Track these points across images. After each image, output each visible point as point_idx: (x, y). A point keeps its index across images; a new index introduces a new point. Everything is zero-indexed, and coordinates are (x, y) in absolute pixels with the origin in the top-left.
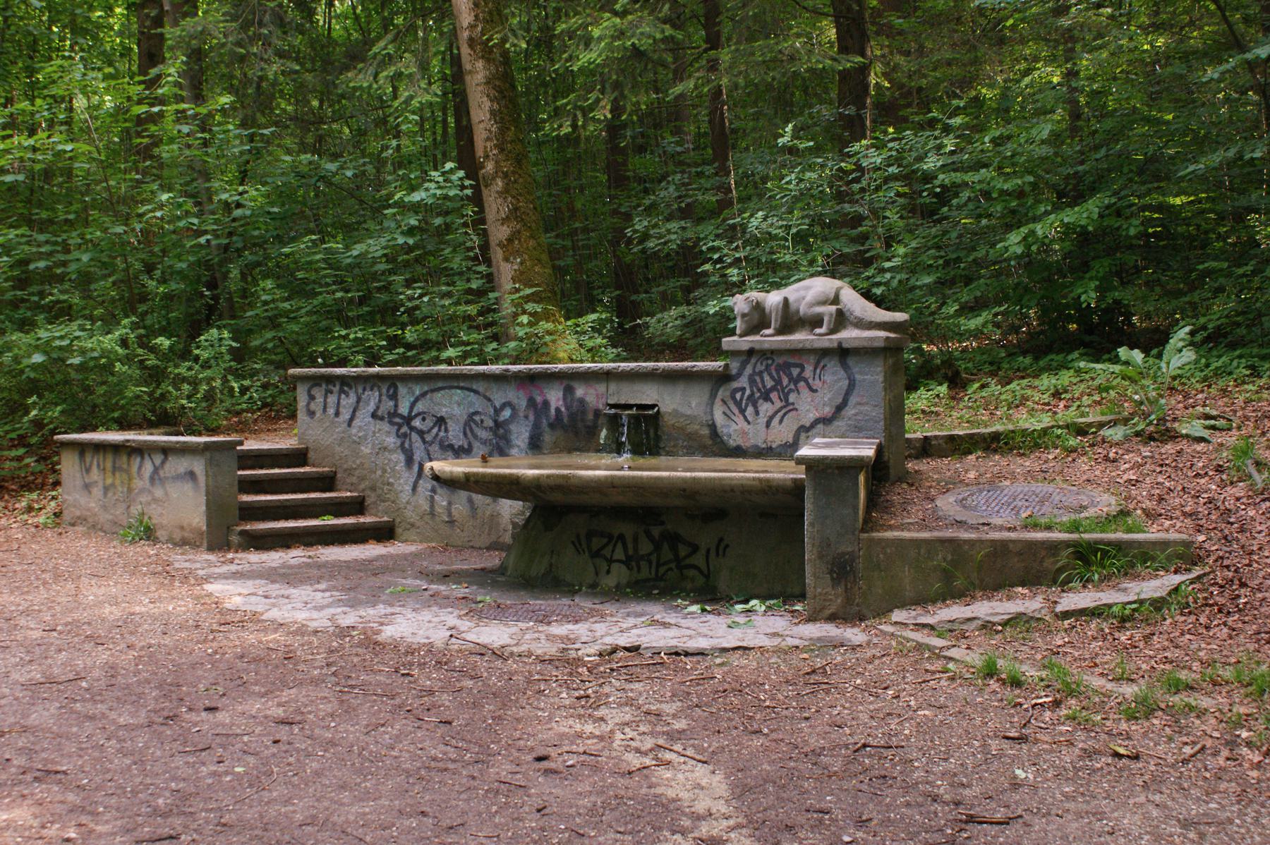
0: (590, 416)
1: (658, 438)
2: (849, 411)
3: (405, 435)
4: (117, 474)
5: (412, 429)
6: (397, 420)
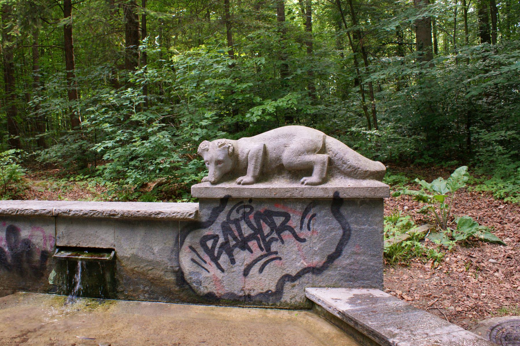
0: (37, 257)
1: (115, 282)
2: (343, 261)
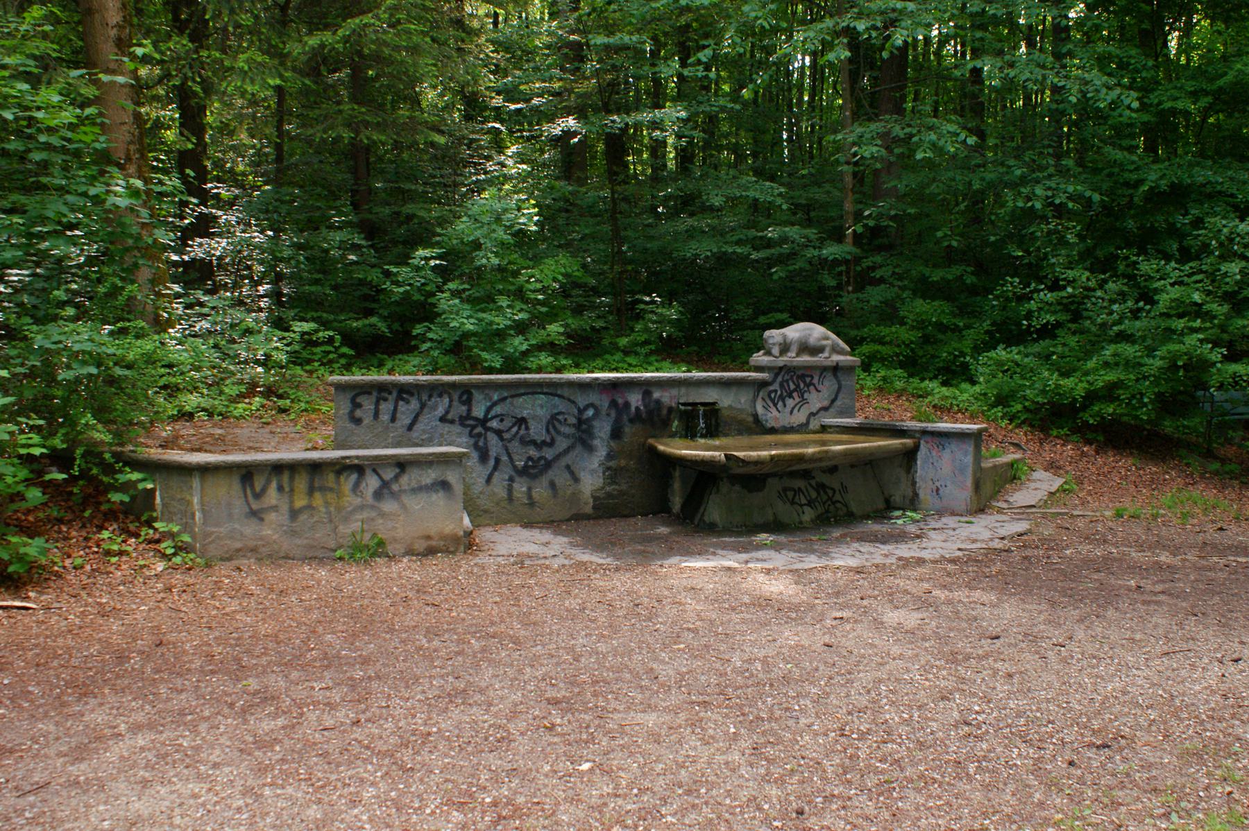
0: (665, 412)
1: (718, 425)
2: (838, 403)
3: (479, 435)
4: (317, 495)
5: (488, 429)
6: (471, 422)
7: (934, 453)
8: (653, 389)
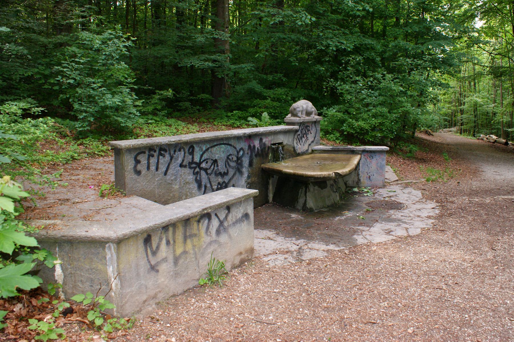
3: (197, 173)
4: (189, 241)
5: (201, 169)
6: (194, 165)
7: (368, 161)
8: (263, 137)
